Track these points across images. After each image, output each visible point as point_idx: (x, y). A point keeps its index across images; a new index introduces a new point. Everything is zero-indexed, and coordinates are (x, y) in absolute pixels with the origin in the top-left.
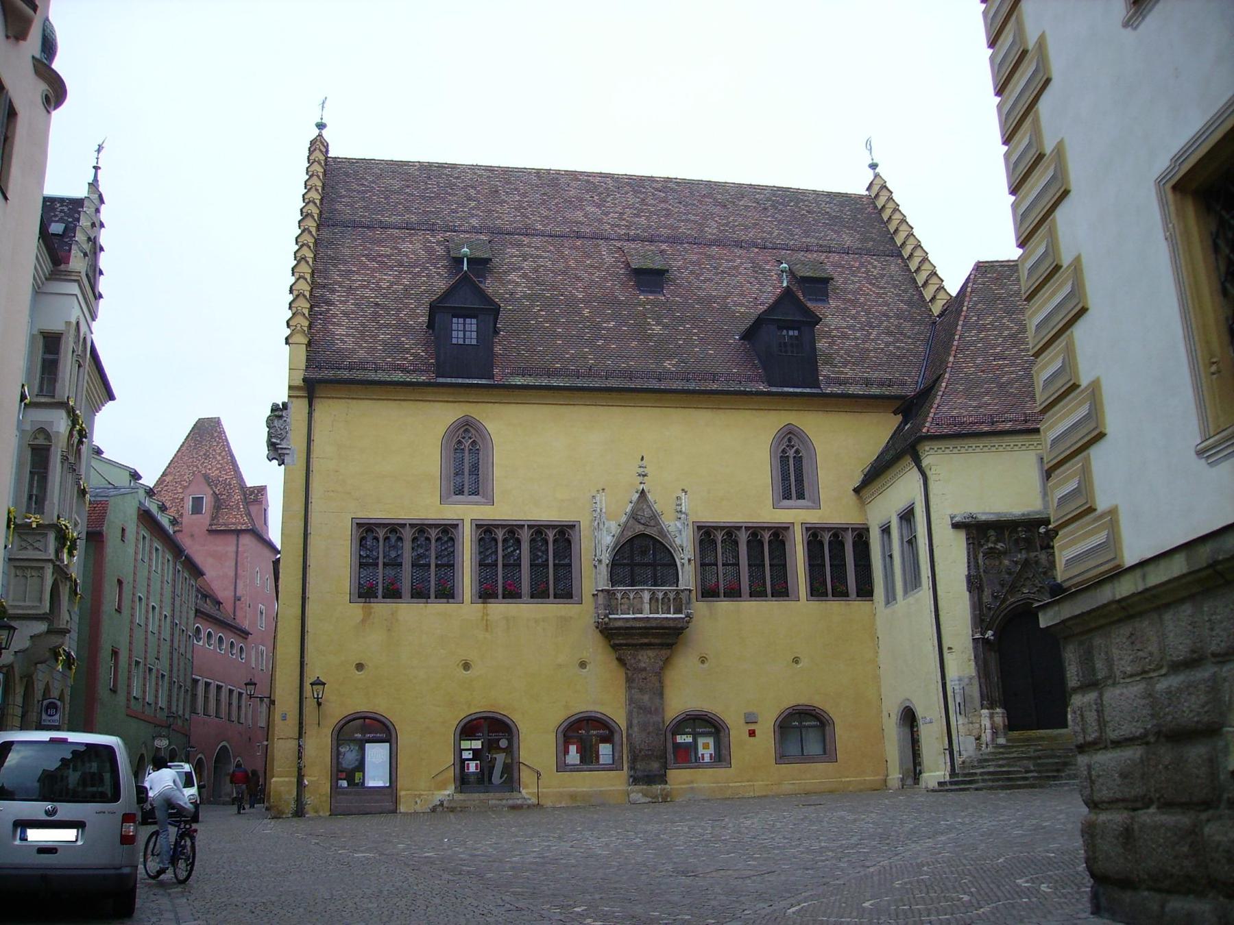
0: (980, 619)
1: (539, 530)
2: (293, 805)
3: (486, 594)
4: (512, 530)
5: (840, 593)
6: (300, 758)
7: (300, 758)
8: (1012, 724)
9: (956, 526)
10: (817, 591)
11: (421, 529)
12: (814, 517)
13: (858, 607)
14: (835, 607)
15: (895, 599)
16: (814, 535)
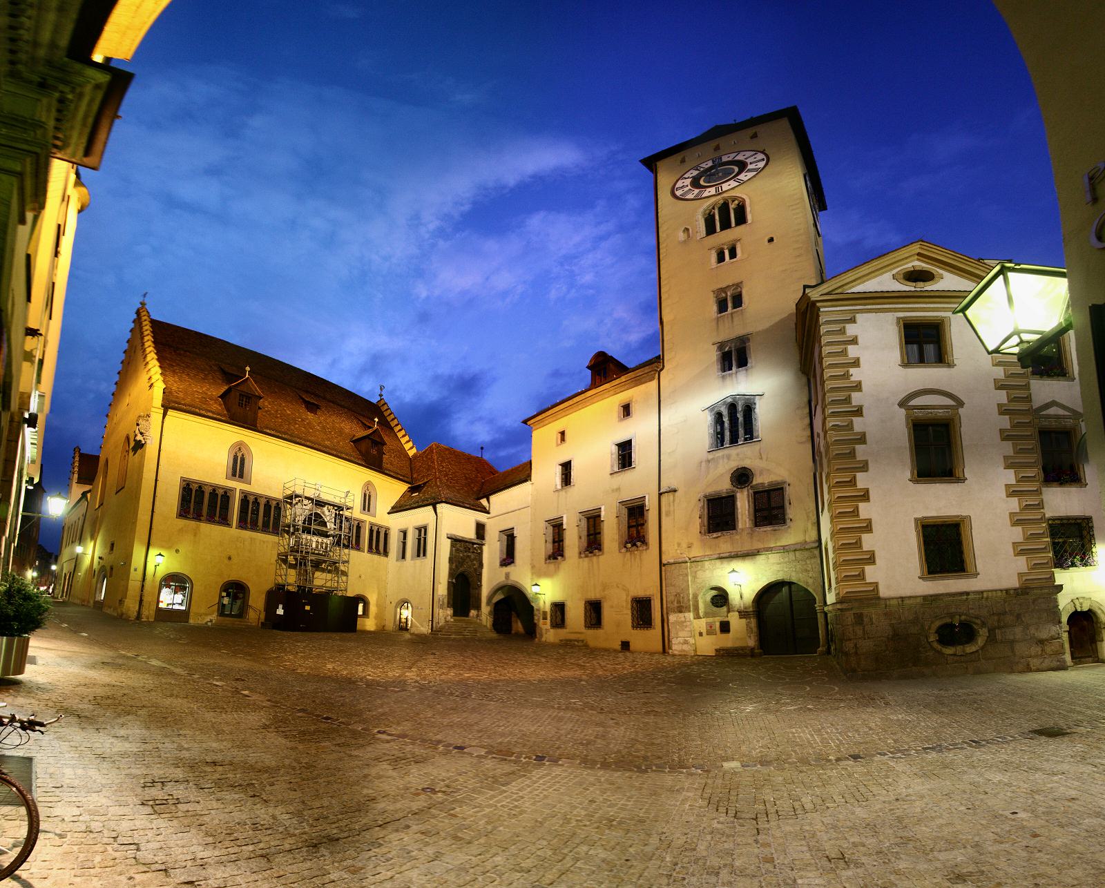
0: (451, 575)
1: (269, 501)
2: (136, 614)
3: (243, 524)
4: (257, 498)
5: (378, 552)
6: (142, 591)
7: (142, 591)
8: (455, 614)
9: (448, 538)
10: (370, 550)
11: (214, 490)
12: (373, 520)
13: (383, 559)
14: (376, 557)
15: (403, 557)
16: (372, 525)
